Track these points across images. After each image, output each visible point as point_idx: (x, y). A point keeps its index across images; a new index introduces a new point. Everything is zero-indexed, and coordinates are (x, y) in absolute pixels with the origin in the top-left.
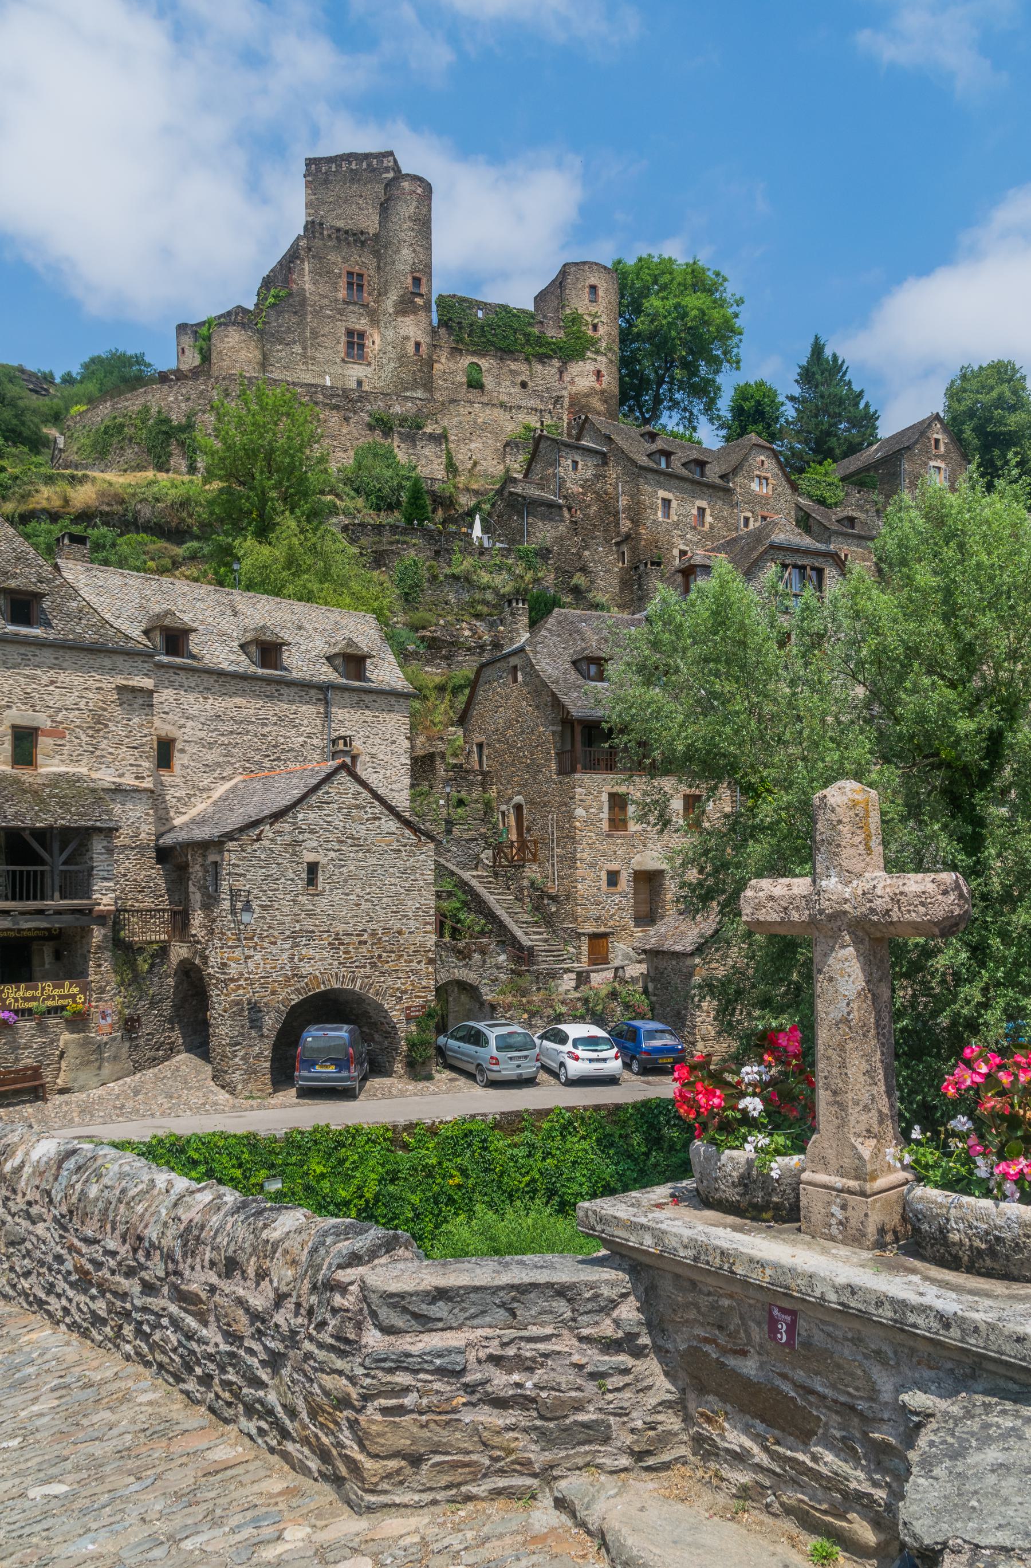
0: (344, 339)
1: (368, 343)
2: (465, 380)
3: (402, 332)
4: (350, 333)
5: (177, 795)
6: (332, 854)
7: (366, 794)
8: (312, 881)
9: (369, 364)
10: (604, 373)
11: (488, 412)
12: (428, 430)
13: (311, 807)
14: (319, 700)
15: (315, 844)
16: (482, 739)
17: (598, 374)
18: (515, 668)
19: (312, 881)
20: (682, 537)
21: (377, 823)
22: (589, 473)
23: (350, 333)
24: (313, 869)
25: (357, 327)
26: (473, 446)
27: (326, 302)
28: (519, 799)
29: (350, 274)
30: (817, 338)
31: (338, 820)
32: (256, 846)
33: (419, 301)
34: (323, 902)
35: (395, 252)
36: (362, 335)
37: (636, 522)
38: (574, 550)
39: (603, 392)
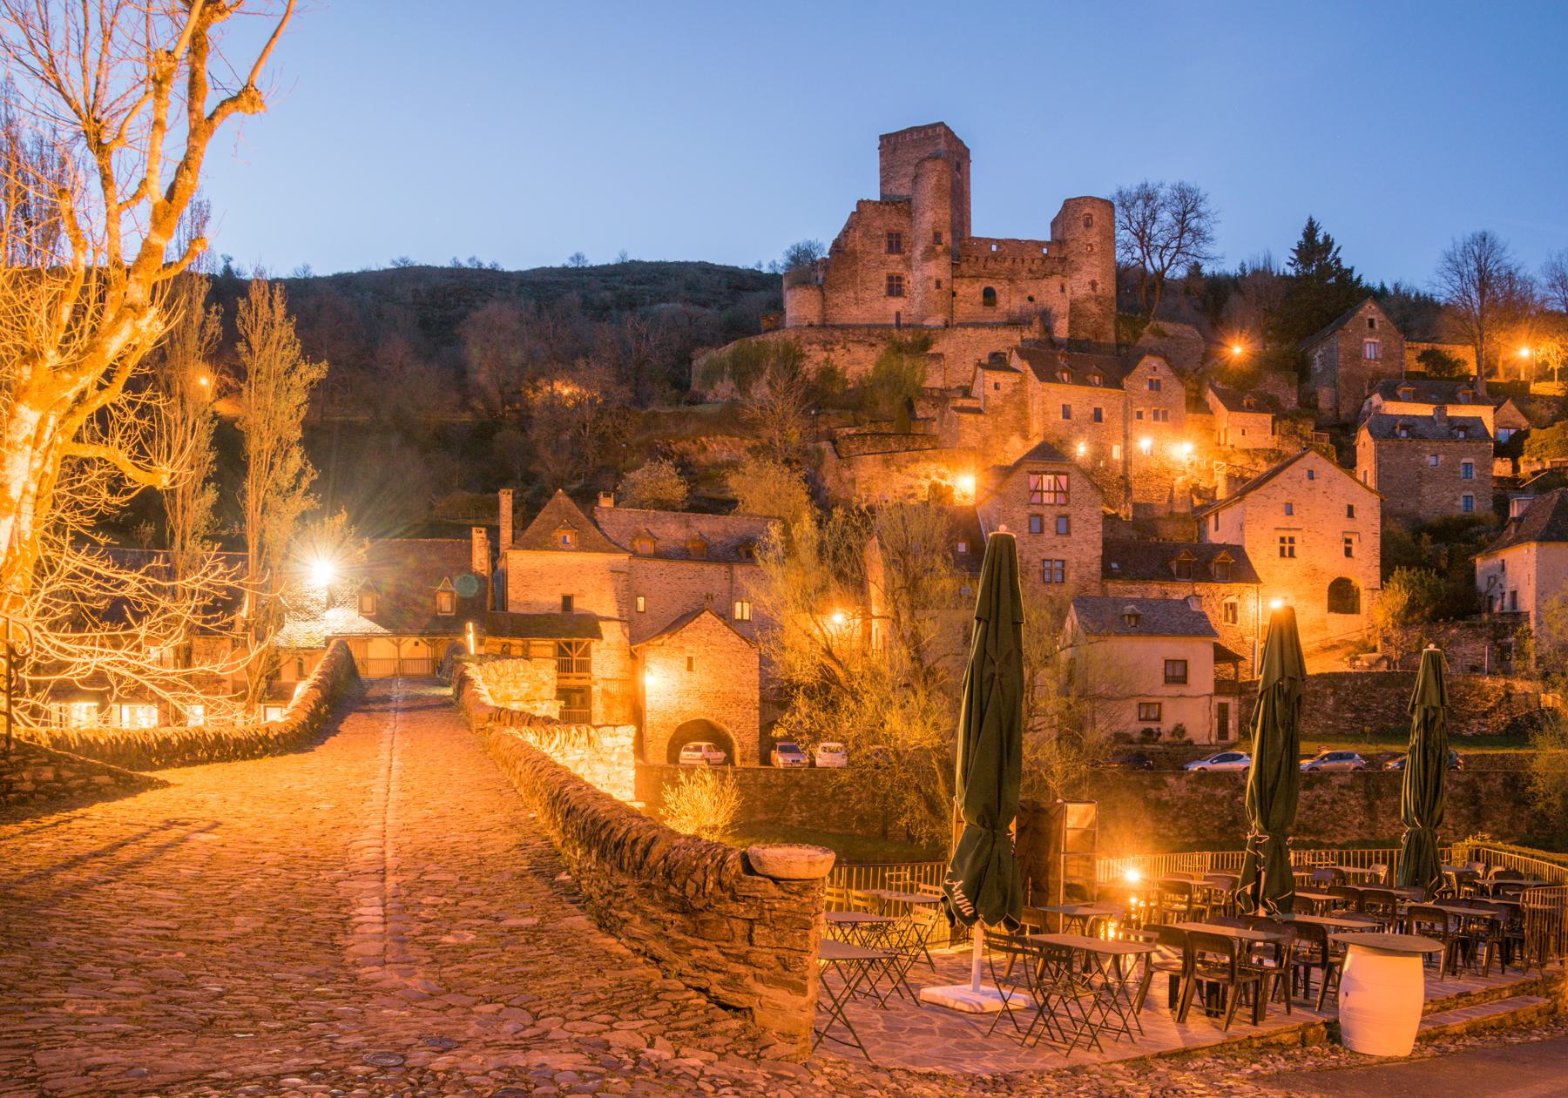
0: (885, 283)
1: (905, 282)
2: (981, 300)
11: (979, 332)
12: (930, 352)
17: (1093, 284)
22: (1008, 391)
23: (890, 278)
30: (1311, 223)
33: (939, 248)
36: (899, 278)
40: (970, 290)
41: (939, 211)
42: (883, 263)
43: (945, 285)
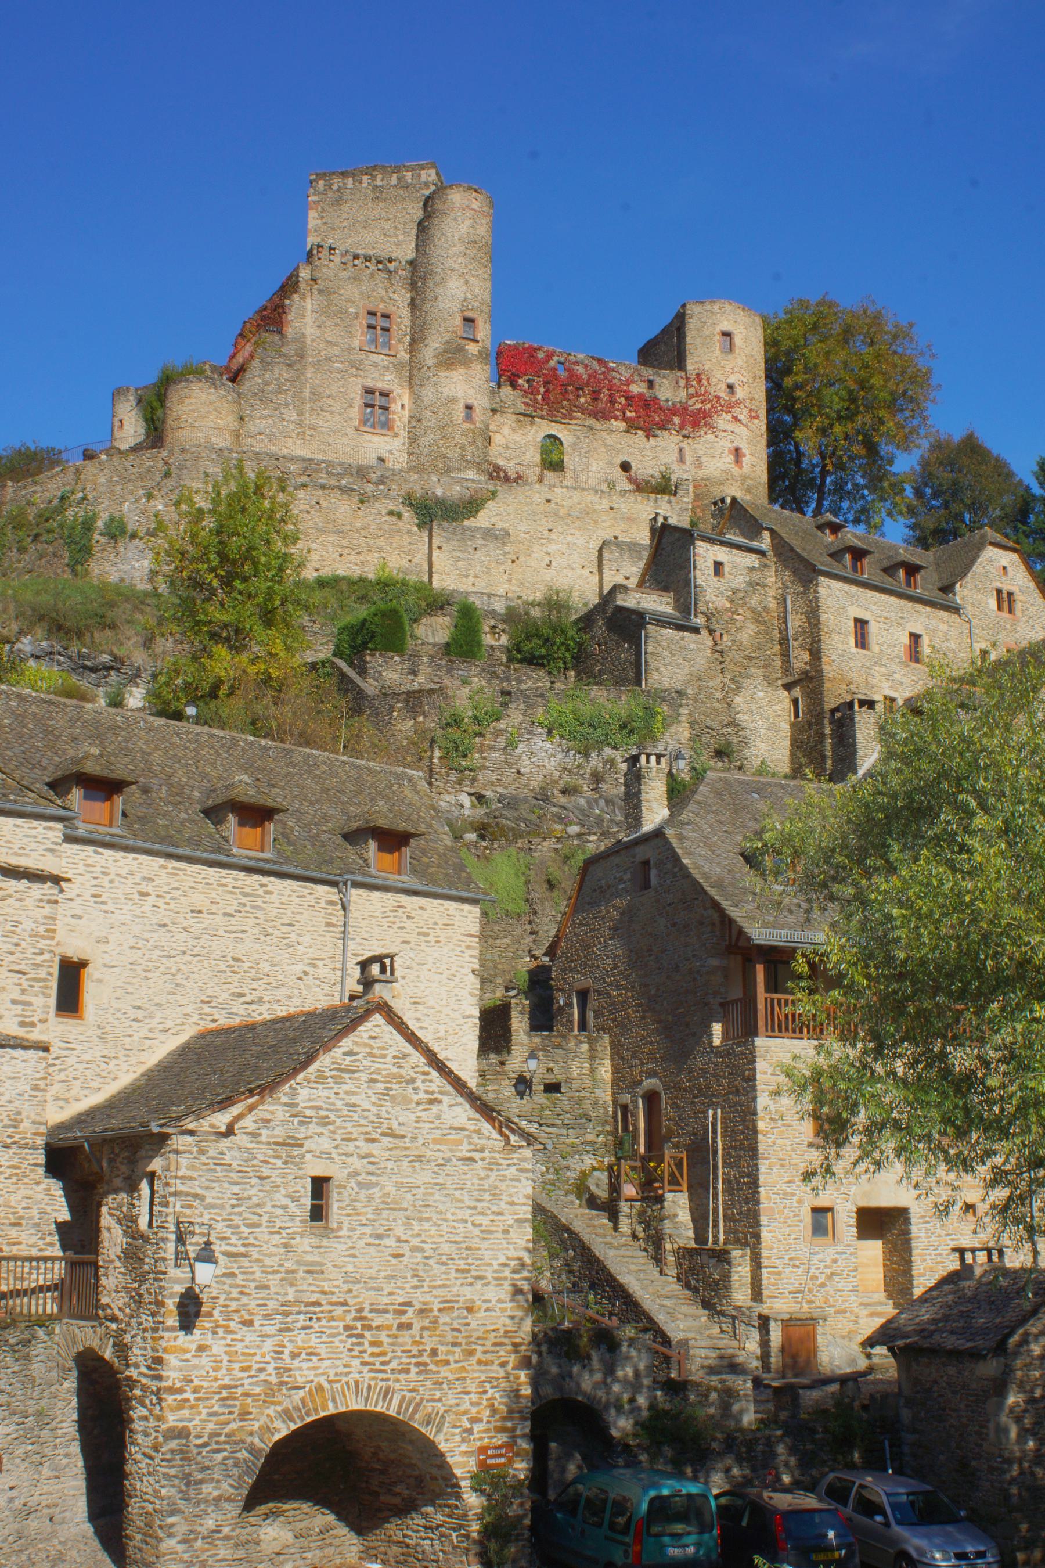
0: (358, 401)
2: (538, 458)
3: (446, 392)
4: (369, 391)
5: (86, 1057)
6: (356, 1163)
7: (417, 1058)
8: (318, 1213)
9: (396, 435)
10: (745, 450)
13: (321, 1078)
14: (331, 903)
15: (325, 1144)
16: (587, 982)
17: (737, 452)
18: (646, 863)
19: (318, 1213)
20: (888, 677)
21: (435, 1108)
22: (740, 581)
24: (320, 1185)
25: (380, 385)
26: (552, 548)
27: (336, 351)
28: (650, 1083)
29: (372, 314)
31: (365, 1100)
32: (226, 1142)
33: (472, 348)
34: (337, 1248)
35: (436, 284)
37: (816, 654)
38: (719, 695)
39: (744, 478)
40: (517, 437)
41: (472, 280)
42: (357, 366)
43: (478, 415)
